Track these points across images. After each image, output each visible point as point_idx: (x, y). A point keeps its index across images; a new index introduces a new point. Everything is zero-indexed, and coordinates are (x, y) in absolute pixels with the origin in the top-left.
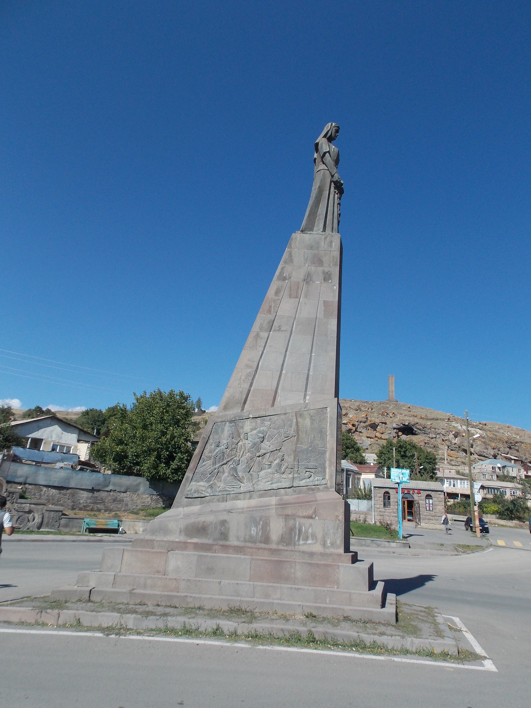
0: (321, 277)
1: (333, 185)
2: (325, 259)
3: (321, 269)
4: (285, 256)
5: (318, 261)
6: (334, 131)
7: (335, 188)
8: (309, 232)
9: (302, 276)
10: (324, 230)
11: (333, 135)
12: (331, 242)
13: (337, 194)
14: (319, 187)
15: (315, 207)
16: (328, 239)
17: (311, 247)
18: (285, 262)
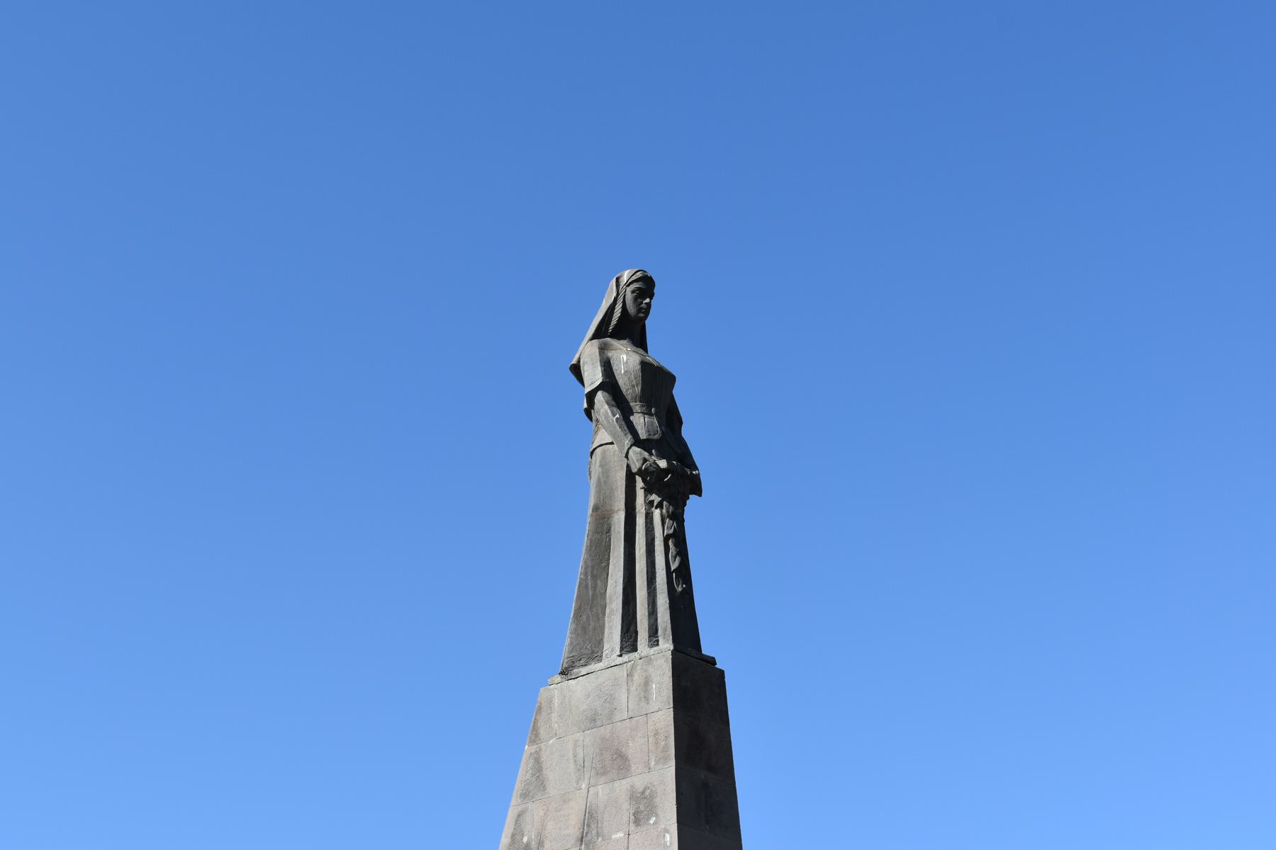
0: (626, 809)
1: (639, 483)
2: (635, 749)
3: (622, 786)
4: (524, 771)
5: (615, 761)
6: (629, 297)
7: (648, 491)
8: (584, 671)
9: (573, 830)
10: (629, 641)
11: (631, 309)
12: (647, 683)
13: (660, 506)
14: (596, 508)
15: (594, 577)
16: (638, 678)
17: (593, 720)
18: (525, 795)
